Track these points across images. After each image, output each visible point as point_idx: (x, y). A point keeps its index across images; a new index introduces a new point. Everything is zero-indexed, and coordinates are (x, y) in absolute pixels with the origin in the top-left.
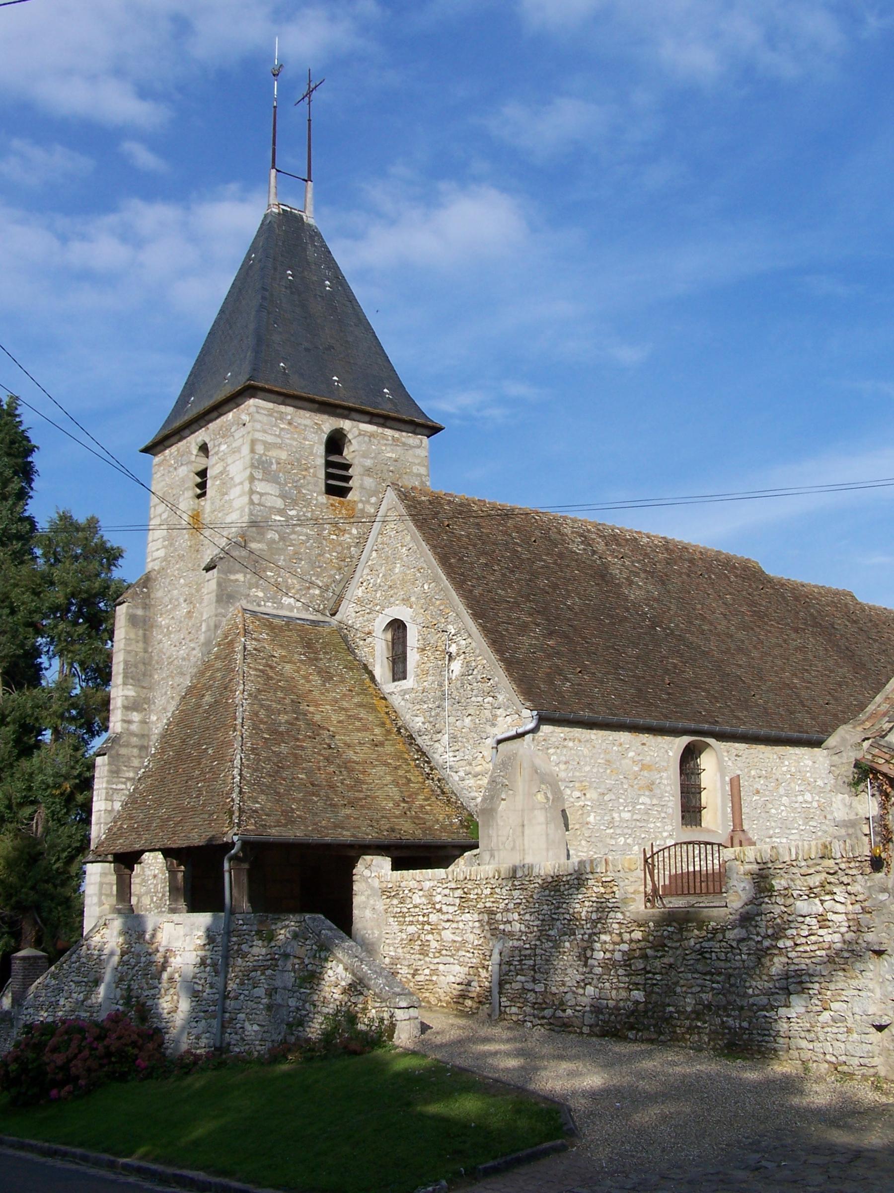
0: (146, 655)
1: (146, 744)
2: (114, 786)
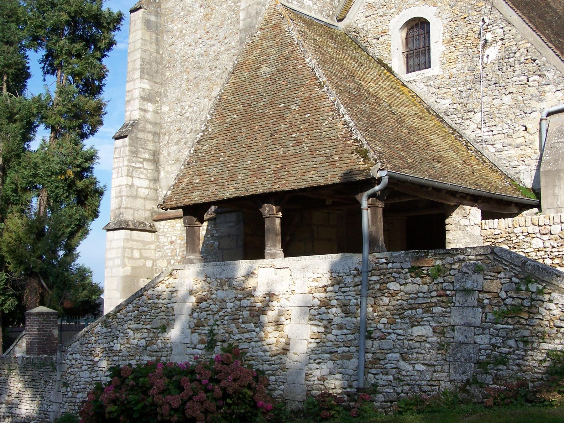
0: (158, 56)
1: (158, 131)
2: (134, 165)
